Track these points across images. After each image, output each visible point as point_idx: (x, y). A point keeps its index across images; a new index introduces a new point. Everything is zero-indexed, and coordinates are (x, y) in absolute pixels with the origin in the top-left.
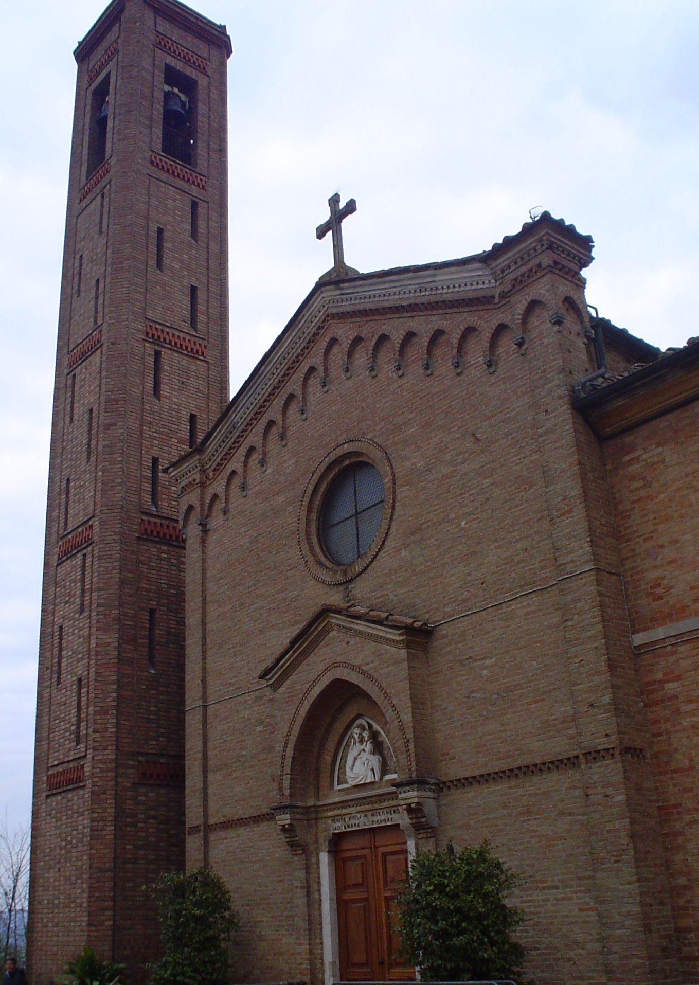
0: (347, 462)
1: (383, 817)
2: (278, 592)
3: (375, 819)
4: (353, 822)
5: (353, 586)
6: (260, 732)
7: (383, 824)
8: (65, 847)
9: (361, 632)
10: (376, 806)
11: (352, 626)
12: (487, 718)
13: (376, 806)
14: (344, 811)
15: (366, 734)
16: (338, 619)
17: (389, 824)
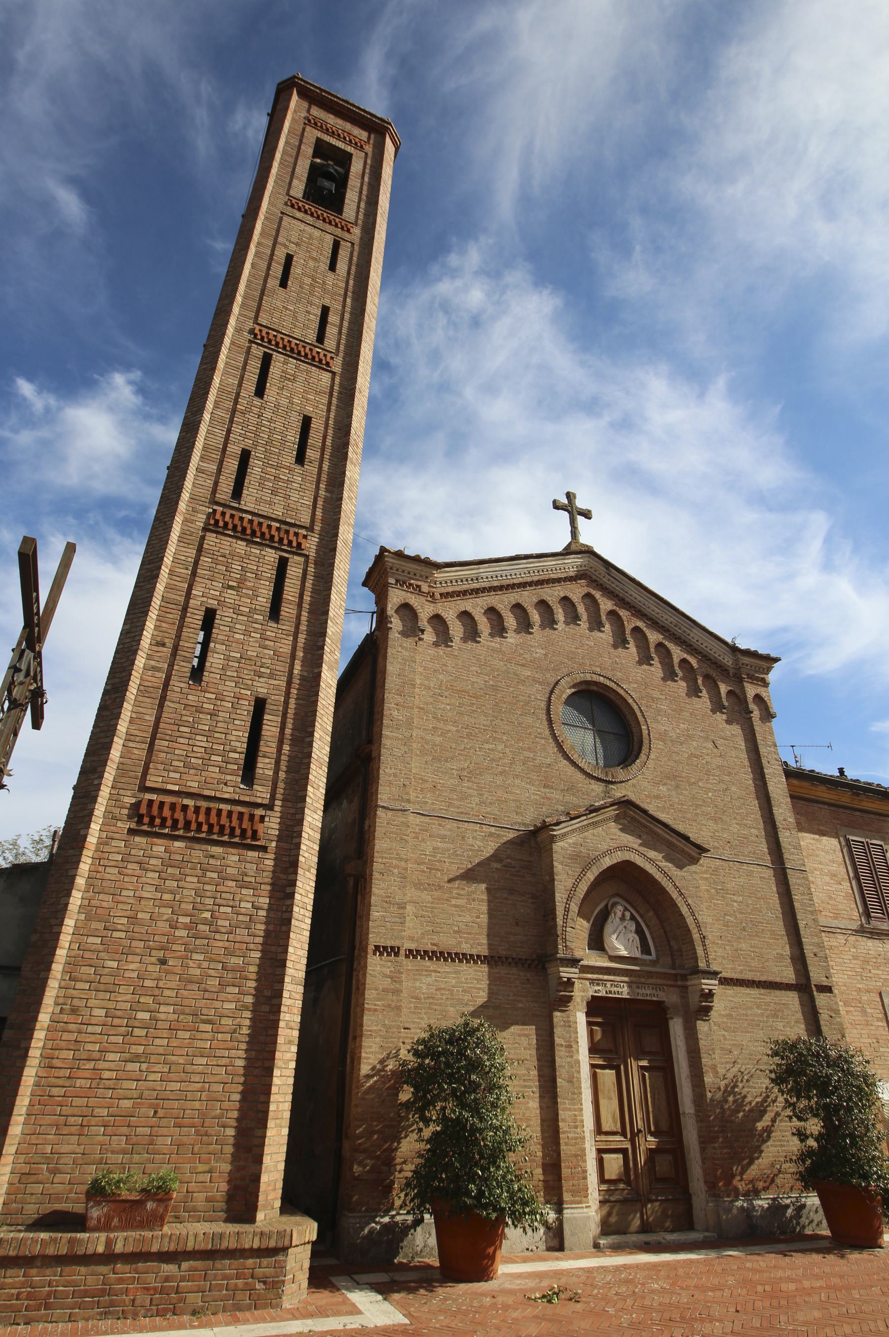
0: (595, 688)
1: (648, 992)
2: (523, 749)
3: (640, 991)
4: (614, 989)
5: (612, 786)
6: (497, 869)
7: (649, 998)
8: (186, 927)
9: (656, 834)
10: (643, 980)
11: (651, 825)
12: (739, 938)
13: (643, 980)
14: (606, 977)
15: (628, 914)
16: (634, 812)
17: (654, 999)
